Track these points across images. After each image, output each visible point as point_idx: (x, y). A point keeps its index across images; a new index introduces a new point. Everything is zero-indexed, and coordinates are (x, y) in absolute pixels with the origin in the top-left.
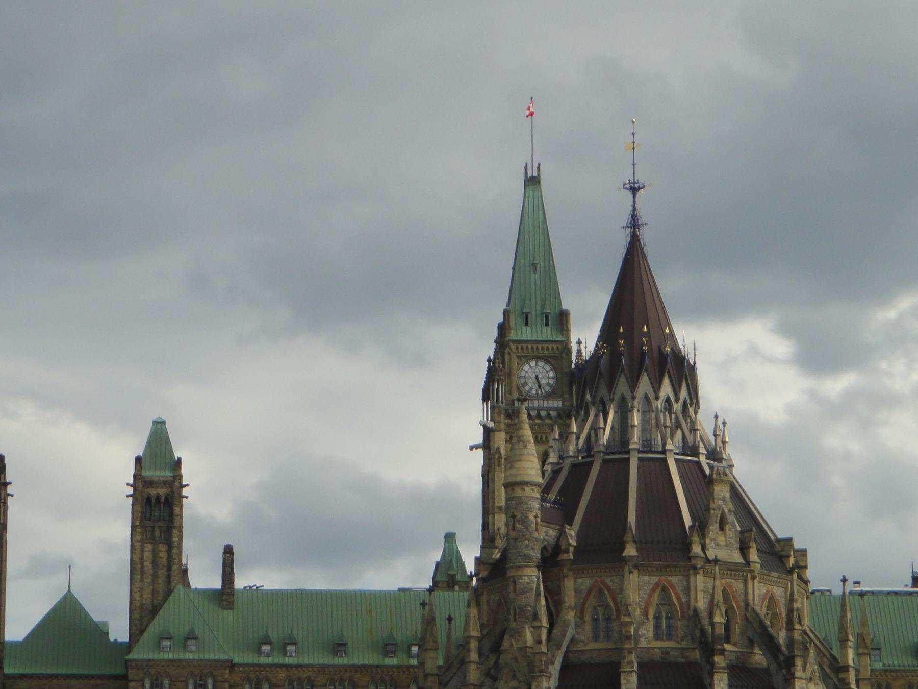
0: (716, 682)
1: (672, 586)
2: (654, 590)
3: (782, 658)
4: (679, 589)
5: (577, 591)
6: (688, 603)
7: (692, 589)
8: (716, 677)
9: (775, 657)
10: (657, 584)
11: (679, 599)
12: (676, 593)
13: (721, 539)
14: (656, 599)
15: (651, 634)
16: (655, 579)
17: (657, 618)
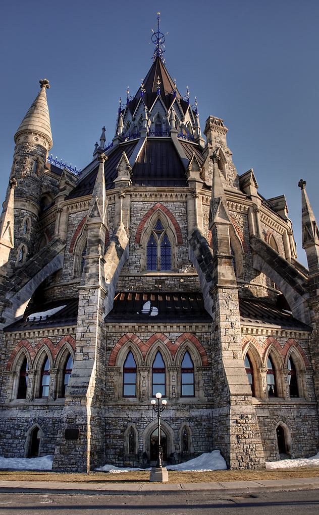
0: (221, 301)
1: (168, 212)
2: (147, 216)
3: (300, 282)
4: (176, 214)
5: (69, 225)
6: (186, 228)
7: (191, 213)
8: (221, 294)
9: (293, 283)
10: (152, 210)
11: (176, 224)
12: (172, 219)
14: (149, 225)
15: (143, 262)
16: (149, 206)
17: (152, 246)
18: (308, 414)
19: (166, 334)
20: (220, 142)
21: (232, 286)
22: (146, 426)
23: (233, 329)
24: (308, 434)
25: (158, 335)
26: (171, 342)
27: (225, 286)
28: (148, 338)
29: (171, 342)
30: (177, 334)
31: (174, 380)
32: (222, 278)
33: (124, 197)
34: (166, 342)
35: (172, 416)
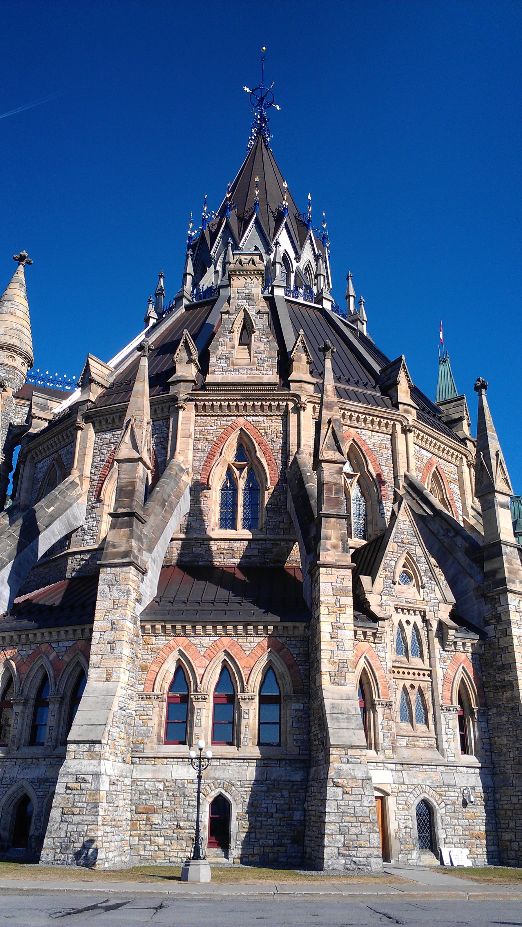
13: (240, 355)
18: (283, 779)
19: (54, 645)
20: (249, 297)
21: (125, 560)
22: (6, 791)
23: (113, 632)
24: (276, 815)
25: (44, 647)
26: (59, 656)
27: (112, 561)
28: (30, 652)
29: (59, 656)
30: (67, 643)
31: (52, 718)
32: (111, 550)
33: (82, 429)
34: (51, 657)
35: (40, 777)
